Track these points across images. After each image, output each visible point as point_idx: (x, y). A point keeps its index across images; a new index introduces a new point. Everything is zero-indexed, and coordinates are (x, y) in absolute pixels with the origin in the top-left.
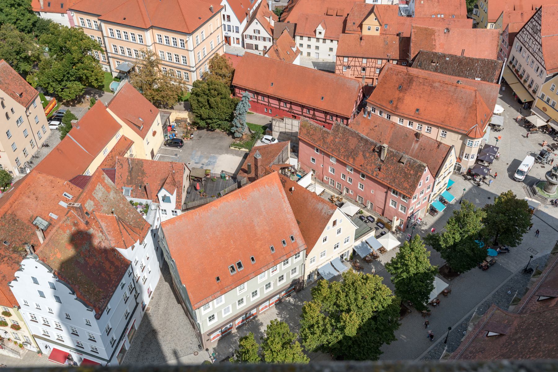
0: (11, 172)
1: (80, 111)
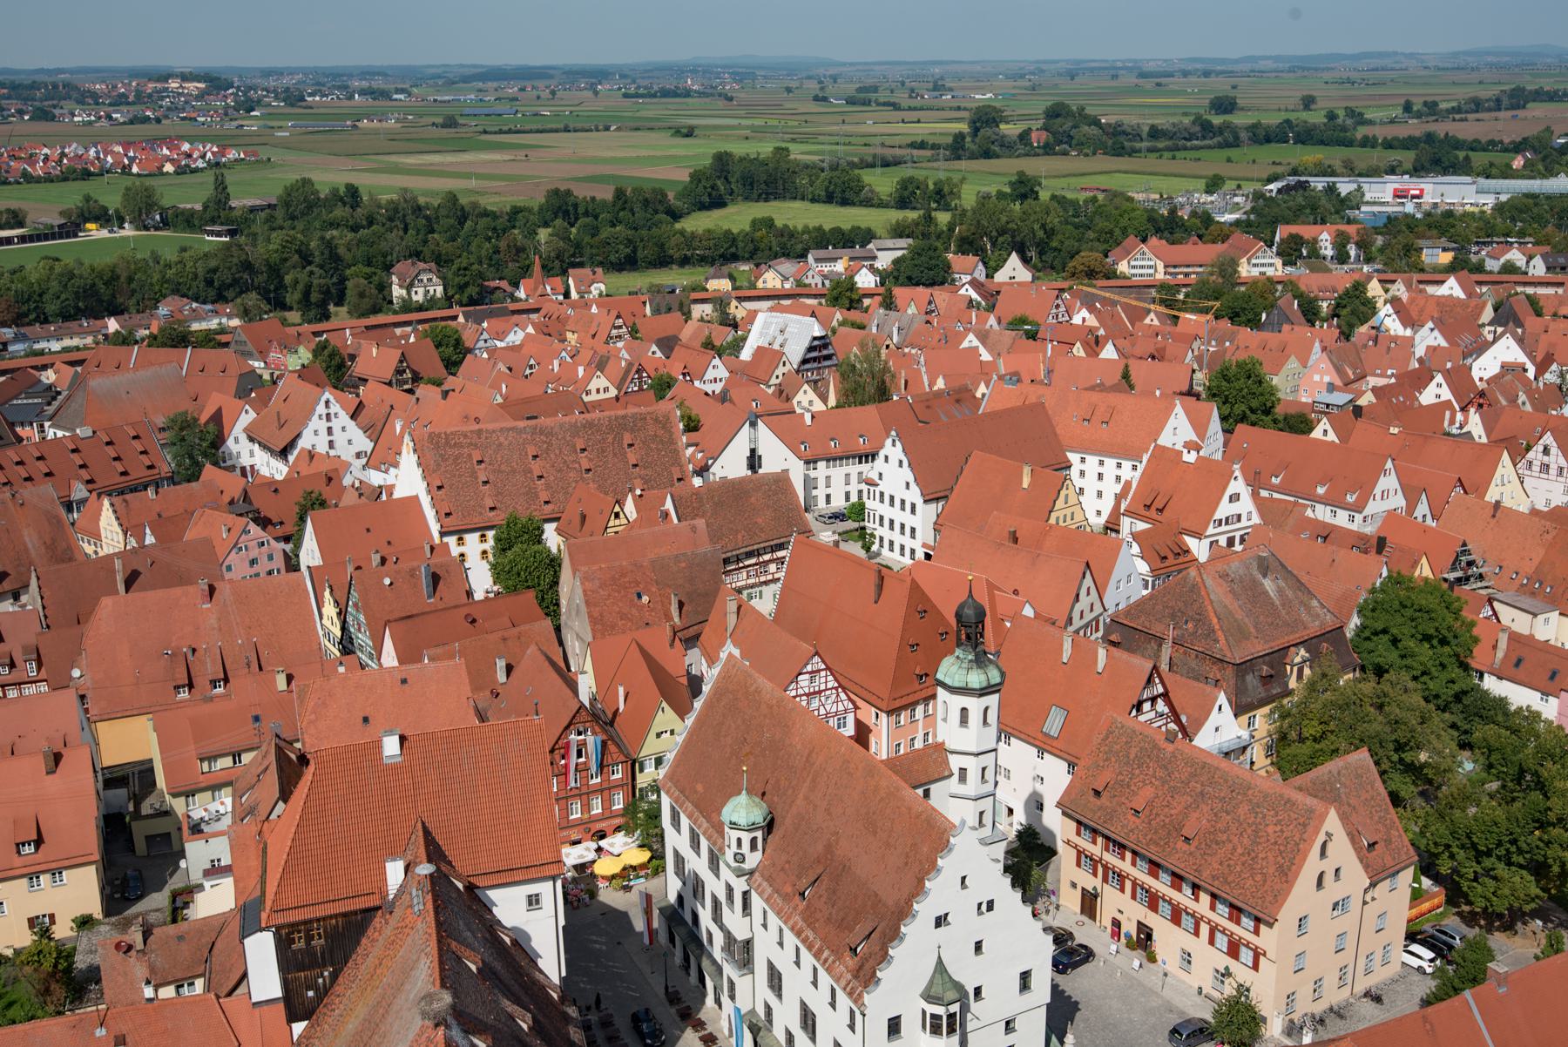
0: (1264, 1020)
1: (1513, 951)
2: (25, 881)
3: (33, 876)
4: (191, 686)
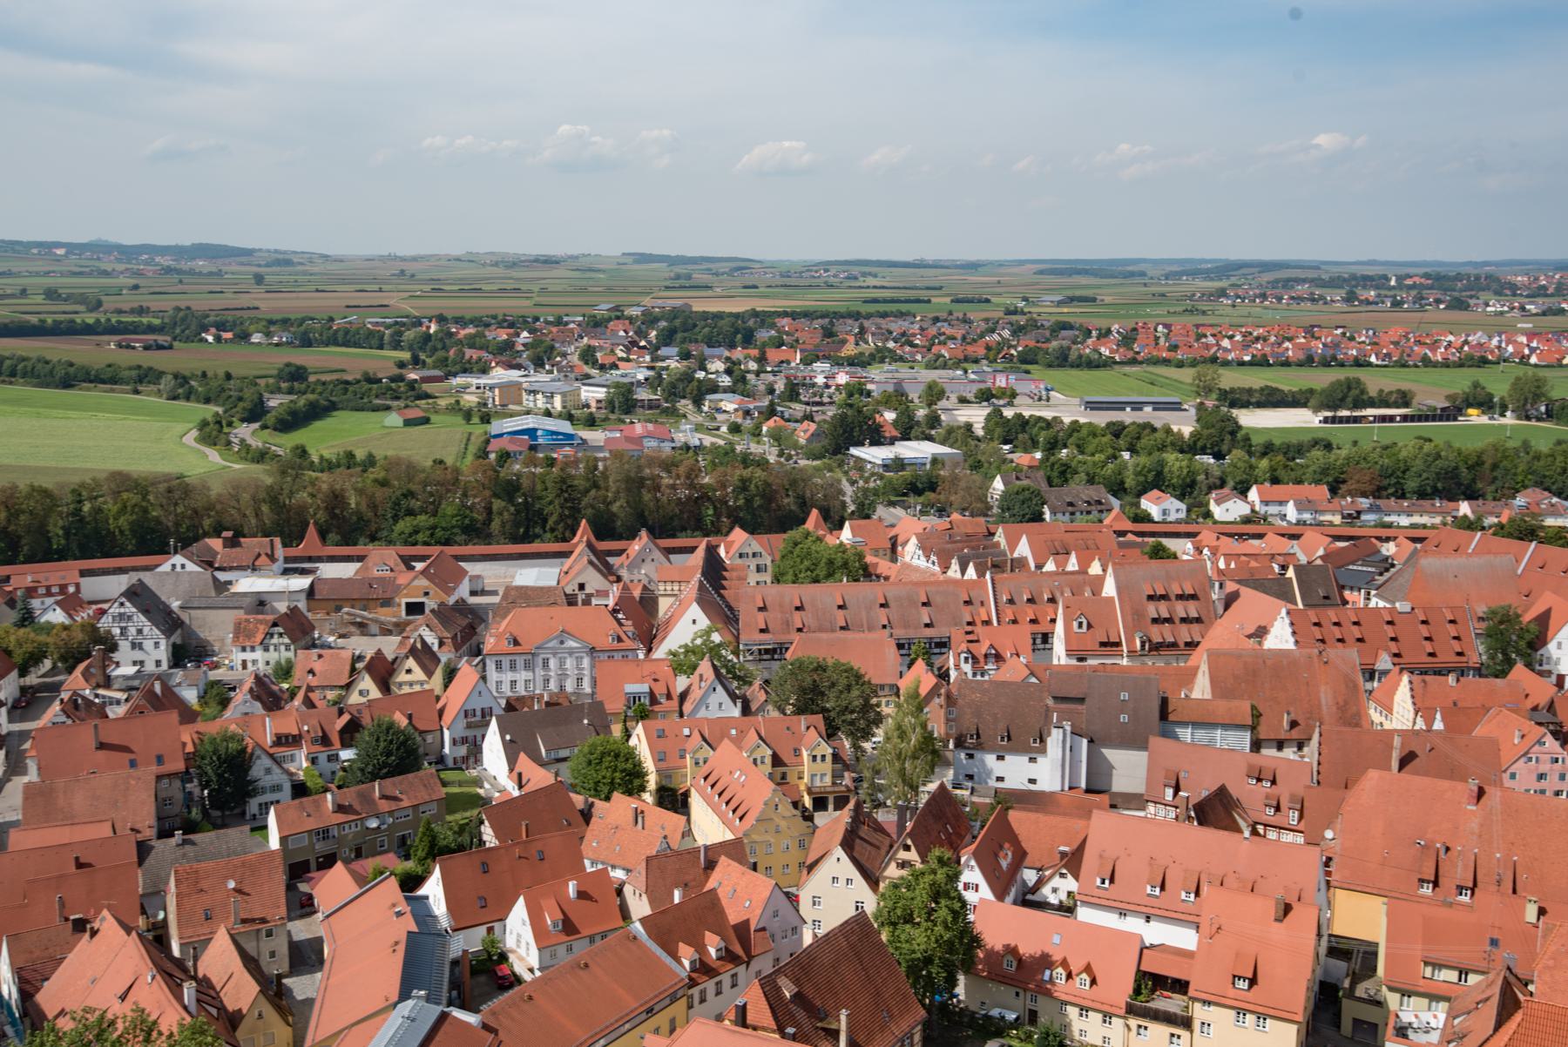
2: (1233, 1013)
3: (1241, 1012)
4: (1436, 884)
